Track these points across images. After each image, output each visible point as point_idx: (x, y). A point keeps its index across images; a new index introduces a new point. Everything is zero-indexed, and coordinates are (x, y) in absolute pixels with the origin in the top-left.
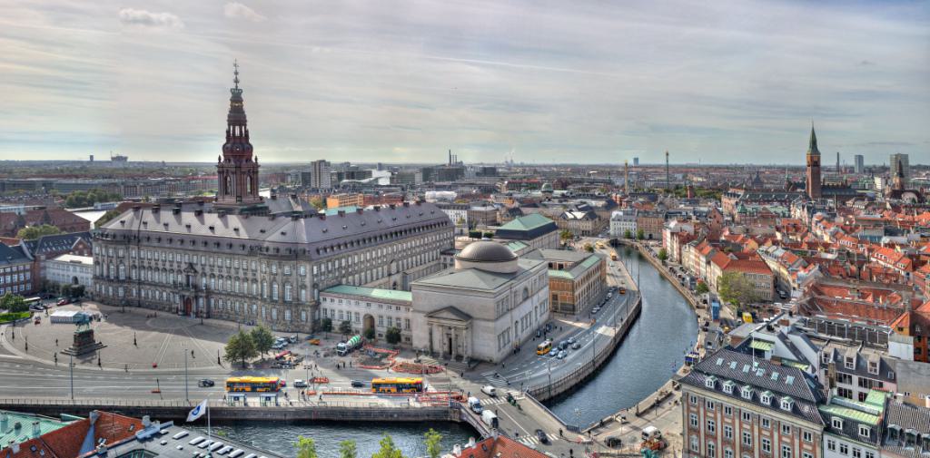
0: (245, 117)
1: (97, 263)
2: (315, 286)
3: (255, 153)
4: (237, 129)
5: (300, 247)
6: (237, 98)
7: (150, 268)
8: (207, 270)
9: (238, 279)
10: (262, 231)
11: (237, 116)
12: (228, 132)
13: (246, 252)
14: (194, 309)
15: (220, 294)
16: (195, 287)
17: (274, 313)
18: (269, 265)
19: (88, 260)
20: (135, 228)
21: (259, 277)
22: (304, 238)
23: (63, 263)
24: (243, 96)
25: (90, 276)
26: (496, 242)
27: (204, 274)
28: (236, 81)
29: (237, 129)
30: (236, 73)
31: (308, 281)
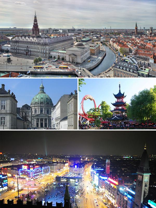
0: (37, 20)
1: (11, 46)
2: (49, 50)
3: (39, 27)
4: (36, 23)
5: (47, 43)
6: (35, 17)
7: (20, 47)
8: (30, 47)
9: (36, 49)
10: (40, 41)
11: (36, 20)
12: (34, 23)
13: (37, 44)
14: (28, 54)
15: (32, 51)
16: (28, 50)
17: (42, 55)
18: (41, 46)
19: (9, 46)
20: (18, 40)
21: (39, 48)
22: (47, 42)
23: (5, 46)
24: (37, 17)
25: (10, 48)
26: (81, 42)
27: (30, 48)
28: (35, 14)
29: (36, 23)
30: (35, 13)
31: (48, 49)
